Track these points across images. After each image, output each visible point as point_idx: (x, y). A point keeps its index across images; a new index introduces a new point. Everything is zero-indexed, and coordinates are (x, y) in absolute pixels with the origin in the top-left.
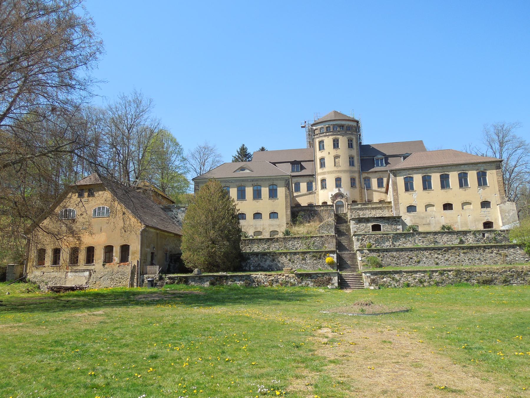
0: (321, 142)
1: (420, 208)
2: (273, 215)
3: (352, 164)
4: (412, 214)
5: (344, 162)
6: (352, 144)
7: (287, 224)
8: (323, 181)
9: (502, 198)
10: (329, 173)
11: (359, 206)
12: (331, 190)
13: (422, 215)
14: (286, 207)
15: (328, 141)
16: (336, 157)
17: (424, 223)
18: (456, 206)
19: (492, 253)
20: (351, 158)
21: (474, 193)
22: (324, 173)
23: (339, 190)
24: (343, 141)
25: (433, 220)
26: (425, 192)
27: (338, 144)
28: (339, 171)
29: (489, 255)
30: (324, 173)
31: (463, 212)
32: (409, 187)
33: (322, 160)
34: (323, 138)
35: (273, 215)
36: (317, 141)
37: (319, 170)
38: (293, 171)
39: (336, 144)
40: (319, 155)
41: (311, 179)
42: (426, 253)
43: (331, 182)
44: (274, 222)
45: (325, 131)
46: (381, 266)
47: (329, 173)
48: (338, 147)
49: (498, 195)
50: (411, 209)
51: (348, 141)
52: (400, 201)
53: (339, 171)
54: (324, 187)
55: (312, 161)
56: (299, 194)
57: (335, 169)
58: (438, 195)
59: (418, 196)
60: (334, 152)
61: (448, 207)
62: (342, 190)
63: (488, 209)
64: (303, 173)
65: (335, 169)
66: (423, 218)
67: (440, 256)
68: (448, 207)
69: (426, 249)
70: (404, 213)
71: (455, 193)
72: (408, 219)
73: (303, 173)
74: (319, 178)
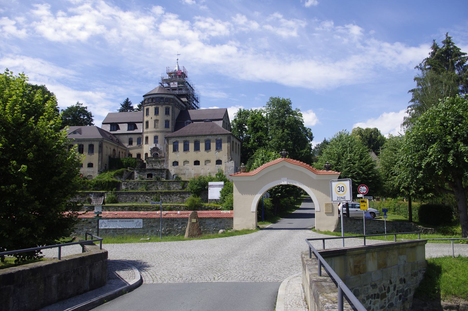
0: (148, 110)
1: (181, 163)
2: (90, 165)
3: (167, 126)
4: (176, 167)
5: (161, 126)
6: (168, 112)
7: (98, 171)
8: (147, 138)
9: (229, 158)
10: (151, 132)
11: (153, 159)
12: (151, 145)
13: (181, 168)
14: (99, 160)
15: (152, 109)
16: (156, 121)
17: (182, 173)
18: (202, 163)
19: (177, 196)
20: (167, 122)
21: (213, 155)
22: (147, 132)
23: (156, 145)
24: (162, 110)
25: (187, 172)
26: (184, 153)
27: (158, 111)
28: (157, 132)
29: (175, 197)
30: (147, 132)
31: (205, 167)
32: (175, 149)
33: (147, 122)
34: (149, 107)
35: (90, 165)
36: (145, 108)
37: (145, 130)
38: (128, 130)
39: (157, 112)
40: (146, 119)
41: (140, 136)
42: (141, 196)
43: (151, 140)
44: (90, 169)
45: (150, 101)
46: (116, 202)
47: (151, 132)
48: (158, 113)
49: (226, 156)
50: (176, 163)
51: (166, 109)
52: (169, 158)
53: (157, 132)
54: (147, 142)
55: (141, 122)
56: (132, 146)
57: (155, 130)
58: (192, 155)
59: (180, 156)
60: (154, 118)
61: (197, 163)
62: (158, 146)
63: (220, 165)
64: (136, 131)
65: (155, 130)
66: (182, 170)
67: (149, 197)
68: (197, 163)
69: (142, 193)
70: (171, 166)
71: (202, 155)
72: (173, 170)
73: (136, 131)
74: (145, 135)
